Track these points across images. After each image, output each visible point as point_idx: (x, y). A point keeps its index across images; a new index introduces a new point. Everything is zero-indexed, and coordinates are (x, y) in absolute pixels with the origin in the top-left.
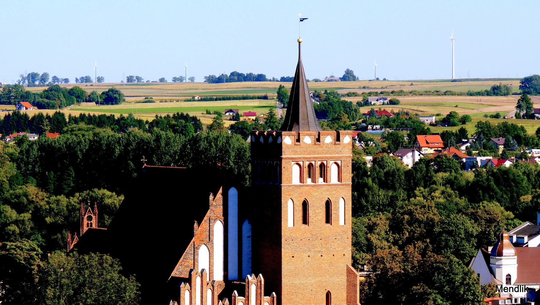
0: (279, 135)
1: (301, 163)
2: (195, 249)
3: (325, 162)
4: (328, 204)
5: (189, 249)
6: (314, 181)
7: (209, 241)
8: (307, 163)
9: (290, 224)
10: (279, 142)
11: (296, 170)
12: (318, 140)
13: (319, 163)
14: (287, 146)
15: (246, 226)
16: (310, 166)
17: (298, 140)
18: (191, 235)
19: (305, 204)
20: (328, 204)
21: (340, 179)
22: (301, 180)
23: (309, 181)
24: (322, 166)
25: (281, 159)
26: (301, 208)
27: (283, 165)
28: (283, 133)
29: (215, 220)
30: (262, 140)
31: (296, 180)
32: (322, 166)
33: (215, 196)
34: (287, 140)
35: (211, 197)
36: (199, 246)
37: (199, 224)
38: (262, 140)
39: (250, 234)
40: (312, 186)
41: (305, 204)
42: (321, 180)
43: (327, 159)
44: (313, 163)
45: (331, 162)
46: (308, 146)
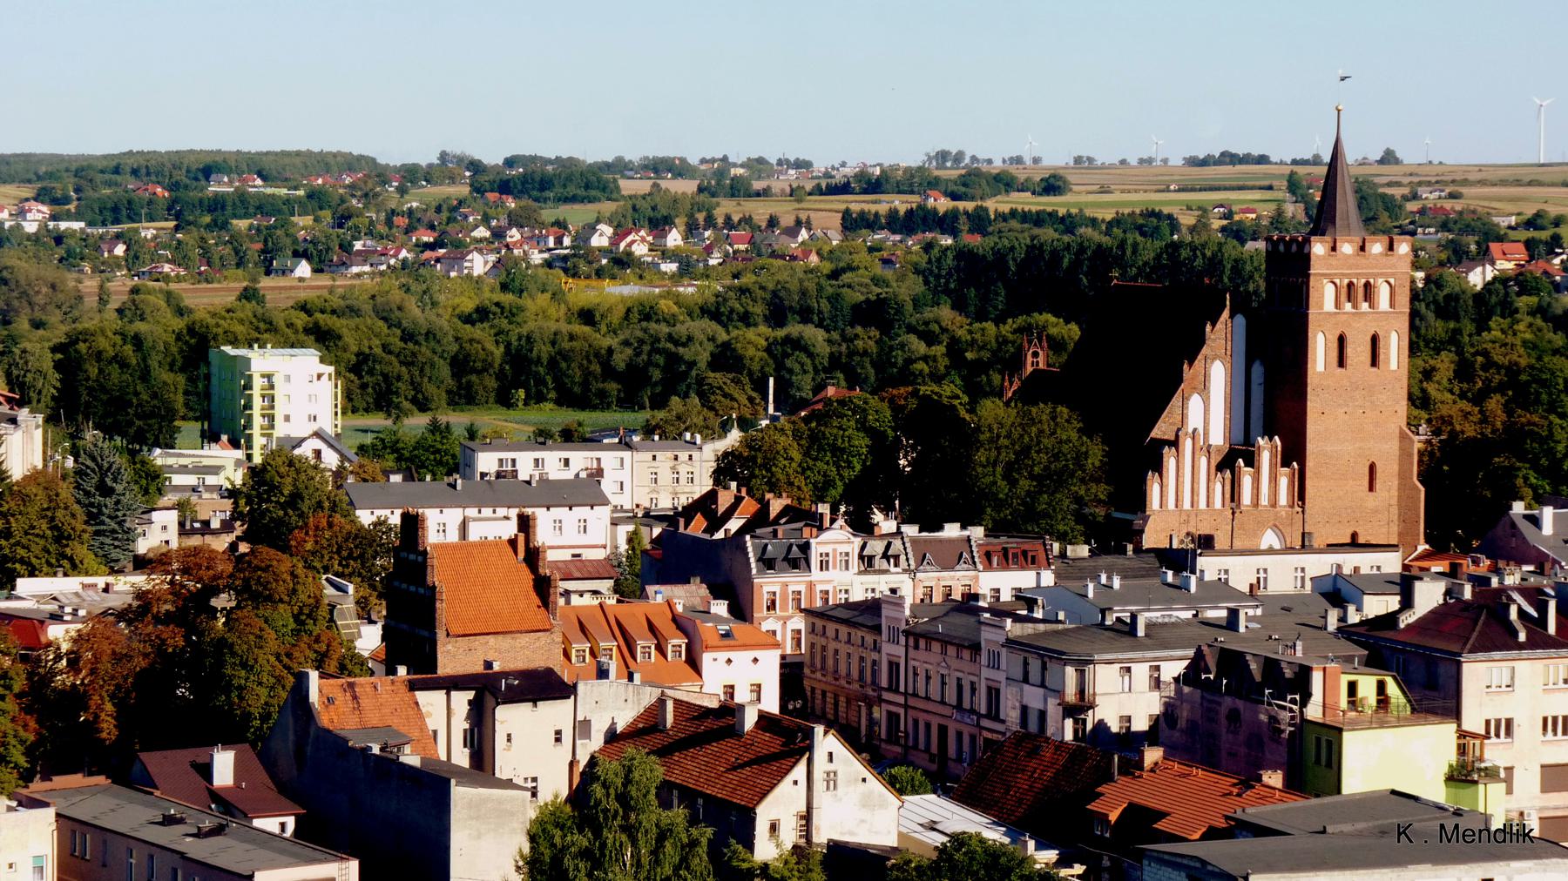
0: (1307, 241)
1: (1337, 281)
2: (1185, 400)
3: (1372, 281)
4: (1375, 340)
5: (1176, 401)
6: (1355, 306)
7: (1204, 389)
8: (1346, 281)
9: (1320, 367)
10: (1306, 251)
11: (1329, 290)
12: (1362, 248)
13: (1363, 281)
14: (1318, 257)
15: (1258, 370)
16: (1350, 285)
17: (1334, 249)
18: (1180, 380)
19: (1342, 340)
20: (1375, 340)
21: (1392, 305)
22: (1338, 305)
23: (1348, 307)
24: (1367, 285)
25: (1309, 275)
26: (1335, 345)
27: (1311, 284)
28: (1313, 238)
29: (1214, 359)
30: (1282, 248)
31: (1329, 305)
32: (1367, 285)
33: (1213, 325)
34: (1318, 248)
35: (1208, 328)
36: (1190, 396)
37: (1191, 365)
38: (1282, 248)
39: (1262, 380)
40: (1353, 314)
41: (1342, 340)
42: (1365, 306)
43: (1376, 276)
44: (1355, 281)
45: (1380, 280)
46: (1348, 257)
